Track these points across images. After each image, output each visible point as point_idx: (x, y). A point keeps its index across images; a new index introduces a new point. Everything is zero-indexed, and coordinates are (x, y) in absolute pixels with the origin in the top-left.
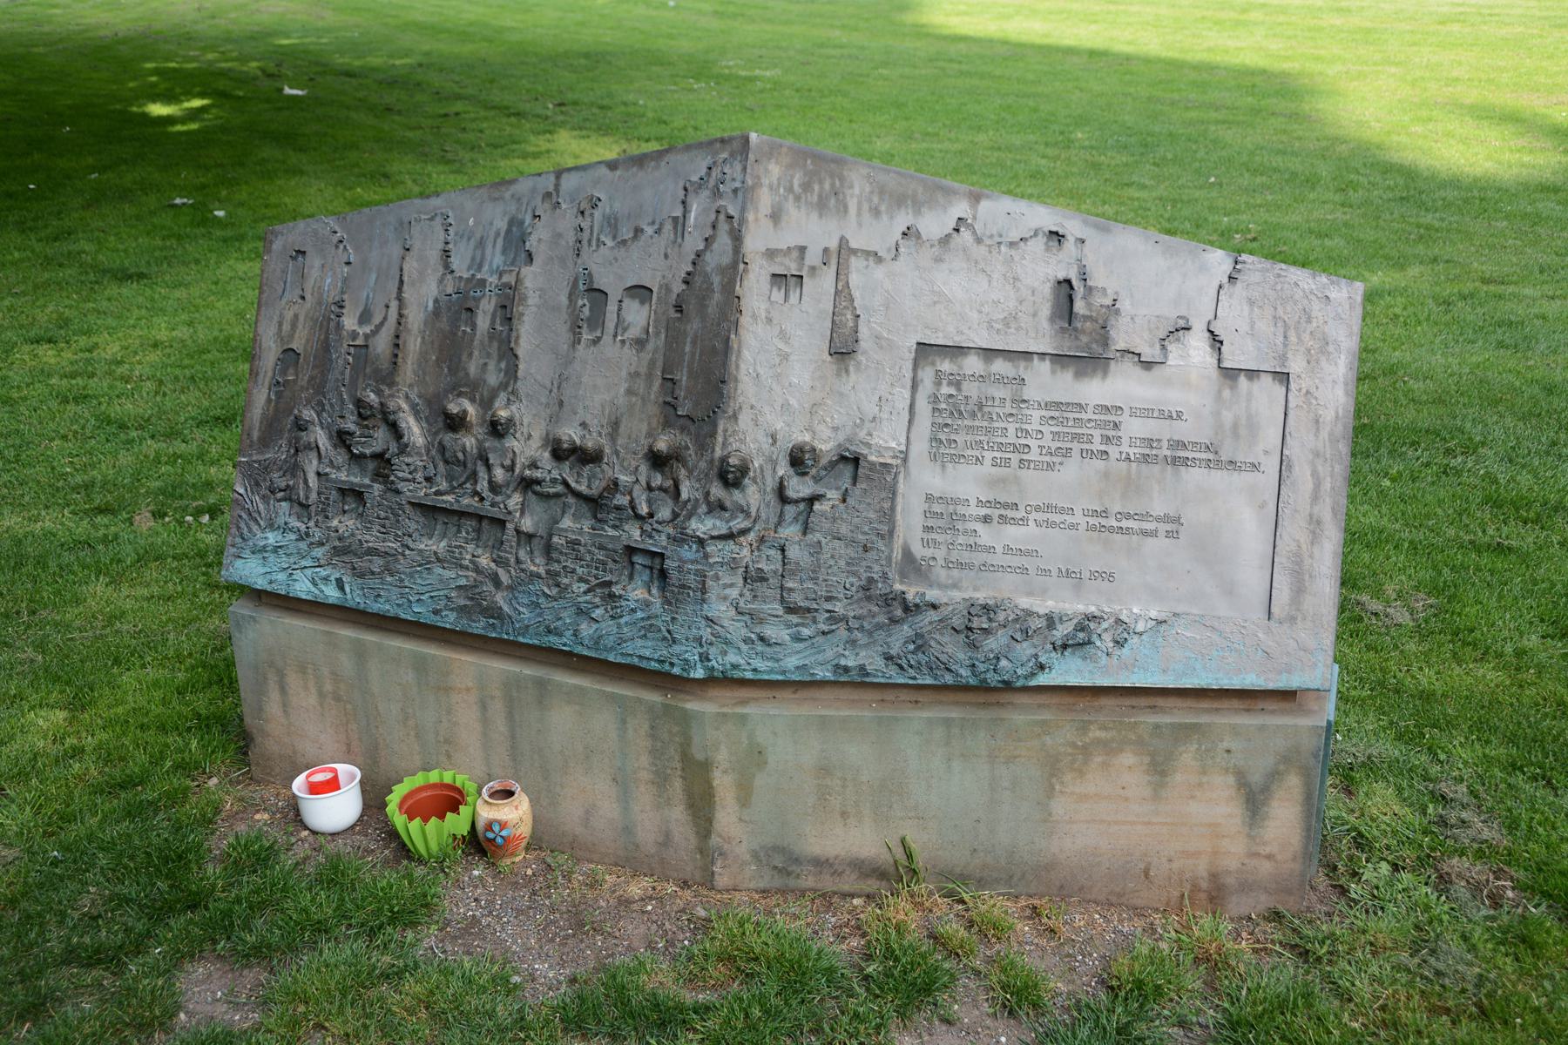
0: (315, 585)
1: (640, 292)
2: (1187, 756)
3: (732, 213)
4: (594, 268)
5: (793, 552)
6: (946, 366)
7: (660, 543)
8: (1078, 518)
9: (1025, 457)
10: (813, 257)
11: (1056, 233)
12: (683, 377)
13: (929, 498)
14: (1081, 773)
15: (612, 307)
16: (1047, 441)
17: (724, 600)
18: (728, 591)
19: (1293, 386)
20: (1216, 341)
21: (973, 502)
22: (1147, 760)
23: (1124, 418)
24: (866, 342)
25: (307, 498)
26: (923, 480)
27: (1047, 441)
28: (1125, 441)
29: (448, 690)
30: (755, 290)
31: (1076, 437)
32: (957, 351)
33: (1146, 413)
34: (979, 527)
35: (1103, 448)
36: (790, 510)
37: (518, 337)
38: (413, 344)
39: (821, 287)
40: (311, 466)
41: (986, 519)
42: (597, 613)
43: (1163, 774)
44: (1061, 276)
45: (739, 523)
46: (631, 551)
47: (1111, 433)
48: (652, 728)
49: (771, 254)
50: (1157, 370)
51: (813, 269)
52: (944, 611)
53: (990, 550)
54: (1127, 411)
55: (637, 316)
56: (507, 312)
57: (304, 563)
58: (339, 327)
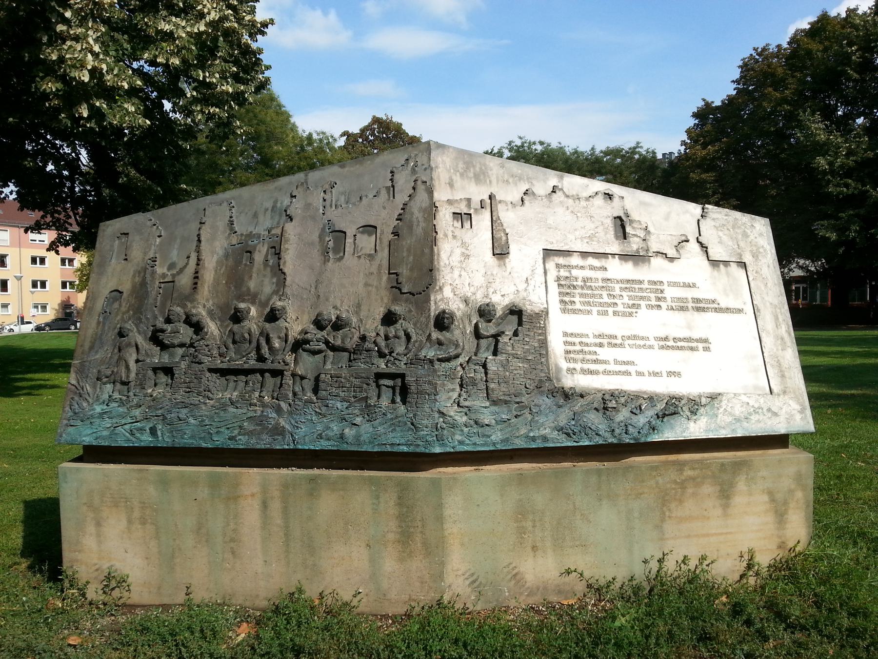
0: (133, 435)
1: (370, 229)
2: (741, 485)
3: (425, 180)
4: (335, 220)
5: (492, 367)
6: (561, 260)
7: (402, 367)
8: (652, 342)
9: (615, 309)
10: (476, 203)
11: (608, 194)
12: (404, 271)
13: (565, 334)
14: (681, 502)
15: (349, 240)
16: (626, 300)
17: (448, 397)
18: (451, 394)
19: (749, 269)
20: (704, 247)
21: (591, 336)
22: (718, 488)
23: (665, 287)
24: (513, 248)
25: (128, 377)
26: (559, 328)
27: (626, 300)
28: (669, 299)
29: (236, 498)
30: (444, 219)
31: (642, 298)
32: (567, 253)
33: (675, 284)
34: (597, 349)
35: (658, 303)
36: (484, 342)
37: (285, 262)
38: (208, 276)
39: (483, 221)
40: (132, 357)
41: (601, 345)
42: (358, 420)
43: (728, 497)
44: (616, 215)
45: (452, 352)
46: (379, 376)
47: (660, 295)
48: (399, 498)
49: (450, 202)
50: (676, 262)
51: (476, 210)
52: (588, 399)
53: (605, 362)
54: (666, 284)
55: (367, 243)
56: (277, 252)
57: (123, 422)
58: (154, 273)
